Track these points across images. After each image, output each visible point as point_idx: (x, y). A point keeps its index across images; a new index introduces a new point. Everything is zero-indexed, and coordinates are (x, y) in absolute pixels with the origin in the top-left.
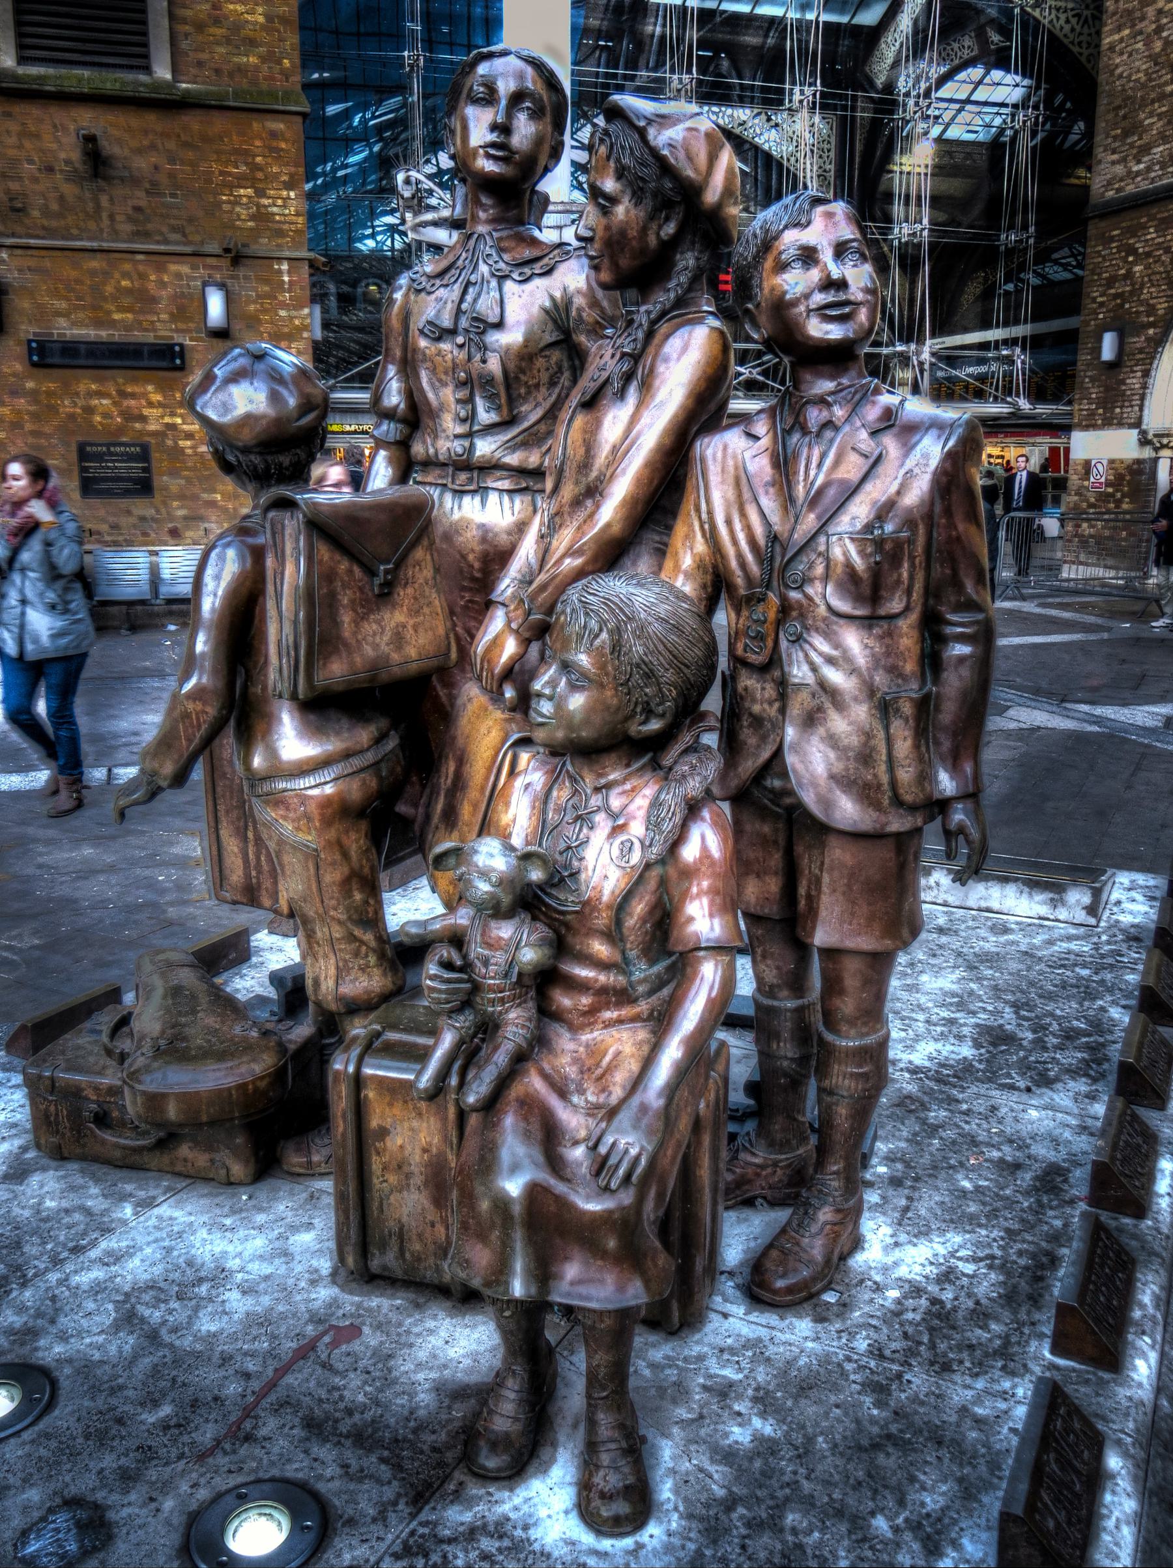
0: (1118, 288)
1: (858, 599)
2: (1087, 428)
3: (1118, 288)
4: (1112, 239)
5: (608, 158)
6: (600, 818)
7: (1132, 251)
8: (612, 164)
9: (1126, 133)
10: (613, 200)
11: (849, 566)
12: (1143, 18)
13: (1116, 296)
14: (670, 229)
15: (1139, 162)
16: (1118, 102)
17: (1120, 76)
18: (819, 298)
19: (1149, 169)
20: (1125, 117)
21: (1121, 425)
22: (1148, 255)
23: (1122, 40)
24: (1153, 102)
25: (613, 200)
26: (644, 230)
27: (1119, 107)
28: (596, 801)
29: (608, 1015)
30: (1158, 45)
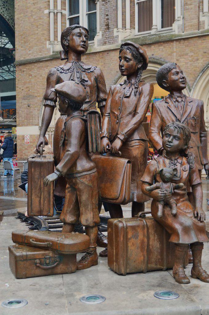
0: (27, 85)
1: (193, 129)
2: (22, 125)
3: (27, 85)
4: (24, 71)
5: (130, 53)
6: (177, 164)
7: (31, 75)
8: (131, 53)
9: (25, 42)
10: (130, 60)
11: (192, 125)
12: (27, 12)
13: (27, 88)
14: (140, 66)
15: (30, 51)
16: (22, 33)
17: (22, 27)
18: (181, 80)
19: (33, 53)
20: (24, 38)
21: (33, 125)
22: (35, 76)
23: (21, 17)
24: (32, 35)
25: (130, 60)
26: (136, 66)
27: (22, 35)
28: (176, 161)
29: (181, 200)
30: (32, 20)
